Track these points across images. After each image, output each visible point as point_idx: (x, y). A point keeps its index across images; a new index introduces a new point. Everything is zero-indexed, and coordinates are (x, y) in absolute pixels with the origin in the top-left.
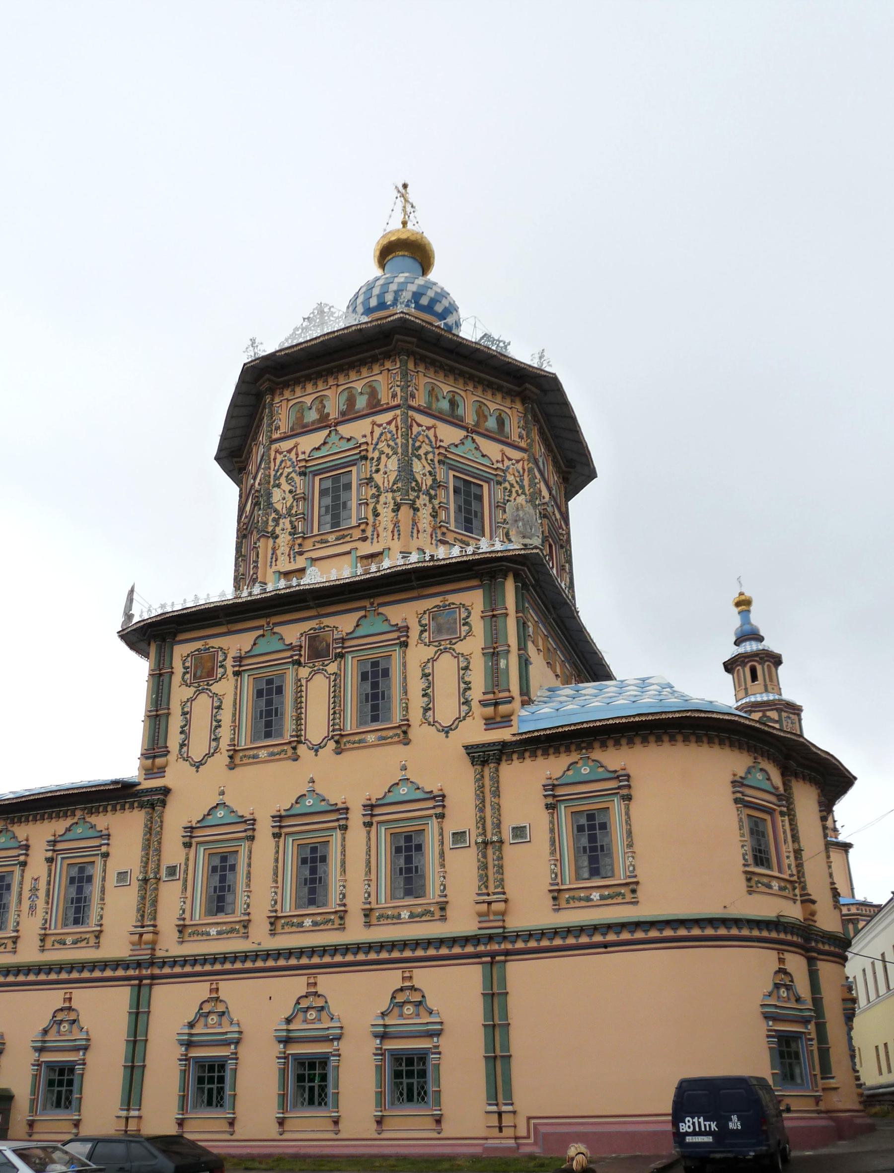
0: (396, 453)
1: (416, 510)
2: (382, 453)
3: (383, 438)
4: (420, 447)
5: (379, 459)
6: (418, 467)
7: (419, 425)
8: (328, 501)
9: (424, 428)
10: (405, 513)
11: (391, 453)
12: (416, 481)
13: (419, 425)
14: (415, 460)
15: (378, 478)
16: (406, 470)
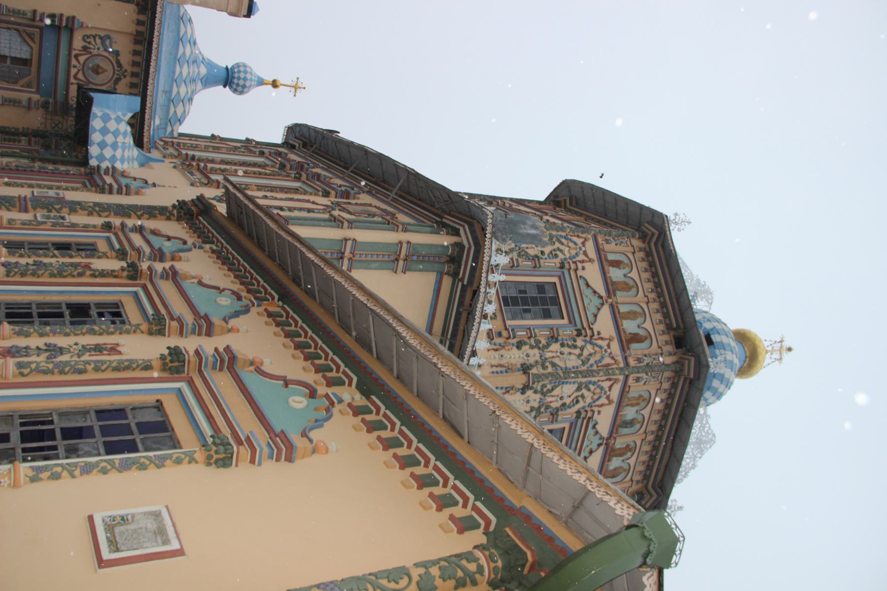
0: (584, 363)
1: (523, 391)
2: (582, 349)
3: (597, 349)
4: (589, 390)
5: (575, 347)
6: (568, 390)
7: (610, 388)
8: (533, 293)
9: (608, 393)
10: (519, 379)
11: (582, 358)
12: (553, 389)
13: (610, 388)
14: (576, 386)
15: (555, 347)
16: (562, 376)
